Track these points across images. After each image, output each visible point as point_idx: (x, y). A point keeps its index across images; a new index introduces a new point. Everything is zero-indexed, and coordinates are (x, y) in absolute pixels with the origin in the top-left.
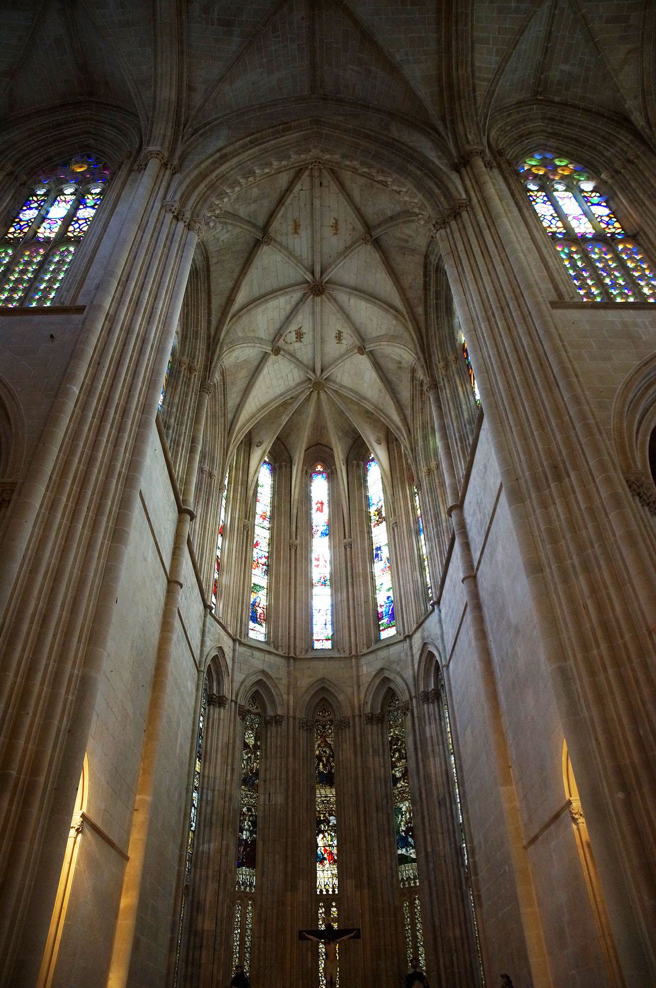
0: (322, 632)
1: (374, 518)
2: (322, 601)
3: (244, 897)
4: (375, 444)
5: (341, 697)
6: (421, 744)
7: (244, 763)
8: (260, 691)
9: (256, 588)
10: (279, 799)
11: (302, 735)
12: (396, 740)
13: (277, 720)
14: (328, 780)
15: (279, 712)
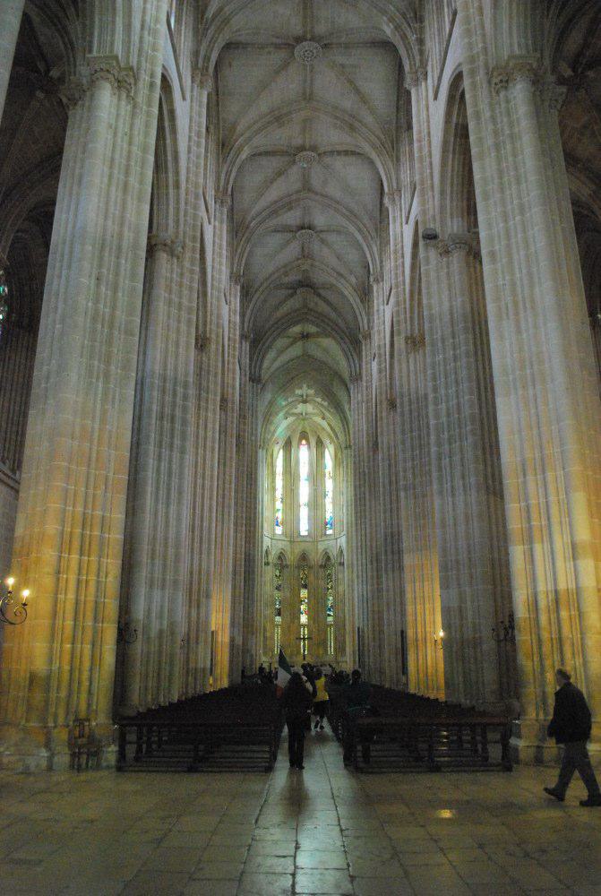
0: (304, 529)
1: (327, 475)
2: (304, 513)
3: (277, 626)
4: (329, 445)
5: (311, 557)
6: (337, 580)
7: (276, 582)
8: (281, 557)
9: (278, 510)
10: (288, 595)
11: (296, 570)
12: (329, 574)
13: (287, 566)
14: (305, 586)
15: (289, 563)
